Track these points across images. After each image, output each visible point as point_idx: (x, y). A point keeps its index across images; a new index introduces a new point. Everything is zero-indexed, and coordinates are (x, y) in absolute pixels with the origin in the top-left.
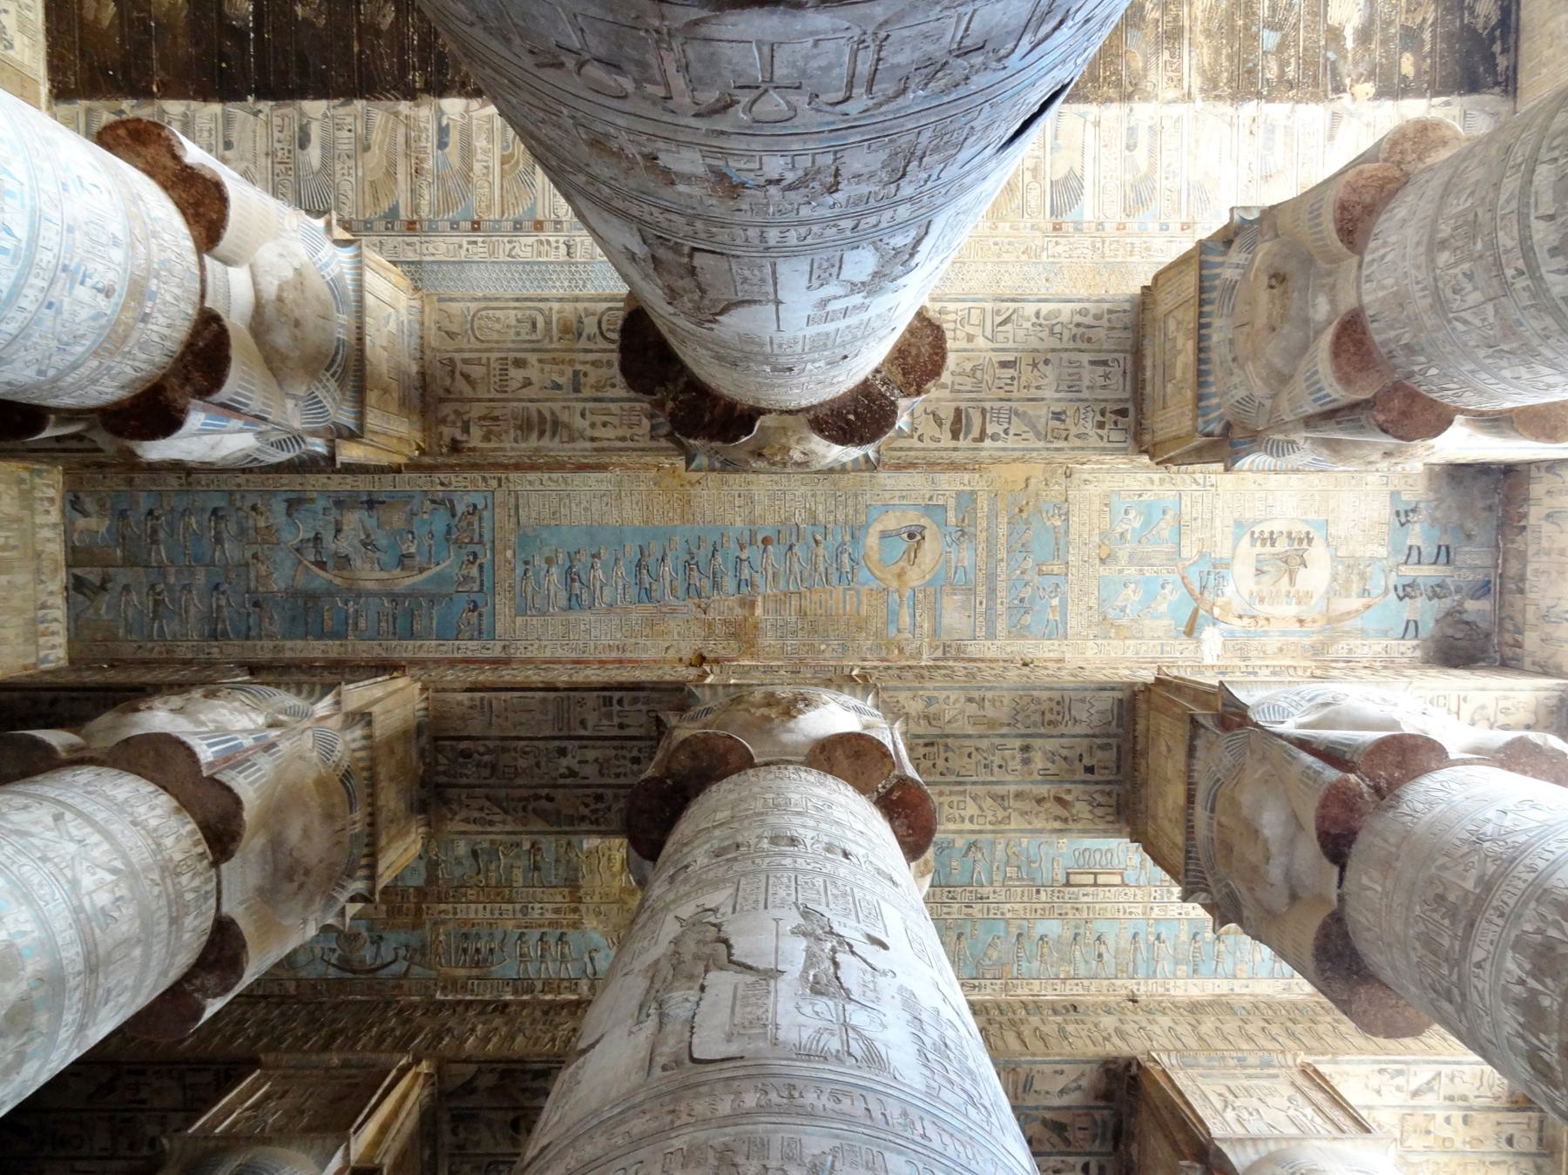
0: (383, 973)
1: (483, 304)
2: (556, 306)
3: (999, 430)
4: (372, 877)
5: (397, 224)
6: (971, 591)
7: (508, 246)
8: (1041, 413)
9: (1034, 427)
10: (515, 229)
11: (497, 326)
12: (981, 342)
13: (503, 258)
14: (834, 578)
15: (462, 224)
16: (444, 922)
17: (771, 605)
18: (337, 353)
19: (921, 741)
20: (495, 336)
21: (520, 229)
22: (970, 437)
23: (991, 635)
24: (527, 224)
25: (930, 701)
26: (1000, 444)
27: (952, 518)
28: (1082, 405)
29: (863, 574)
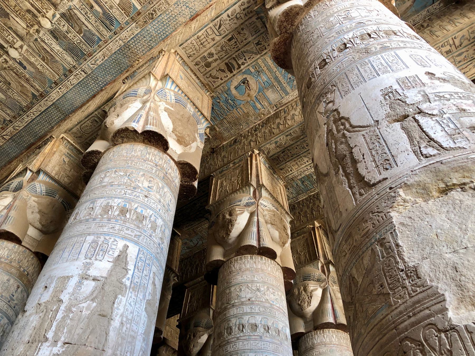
0: (198, 245)
1: (80, 125)
2: (96, 113)
3: (243, 60)
4: (174, 272)
5: (38, 97)
6: (272, 86)
7: (69, 83)
8: (252, 46)
9: (253, 53)
10: (66, 77)
11: (88, 128)
12: (218, 38)
13: (71, 87)
14: (231, 108)
15: (52, 85)
16: (202, 231)
17: (219, 126)
18: (64, 205)
19: (280, 153)
20: (91, 130)
21: (67, 76)
22: (236, 69)
23: (287, 94)
24: (67, 73)
25: (276, 143)
26: (246, 65)
27: (253, 70)
28: (263, 35)
29: (238, 103)
